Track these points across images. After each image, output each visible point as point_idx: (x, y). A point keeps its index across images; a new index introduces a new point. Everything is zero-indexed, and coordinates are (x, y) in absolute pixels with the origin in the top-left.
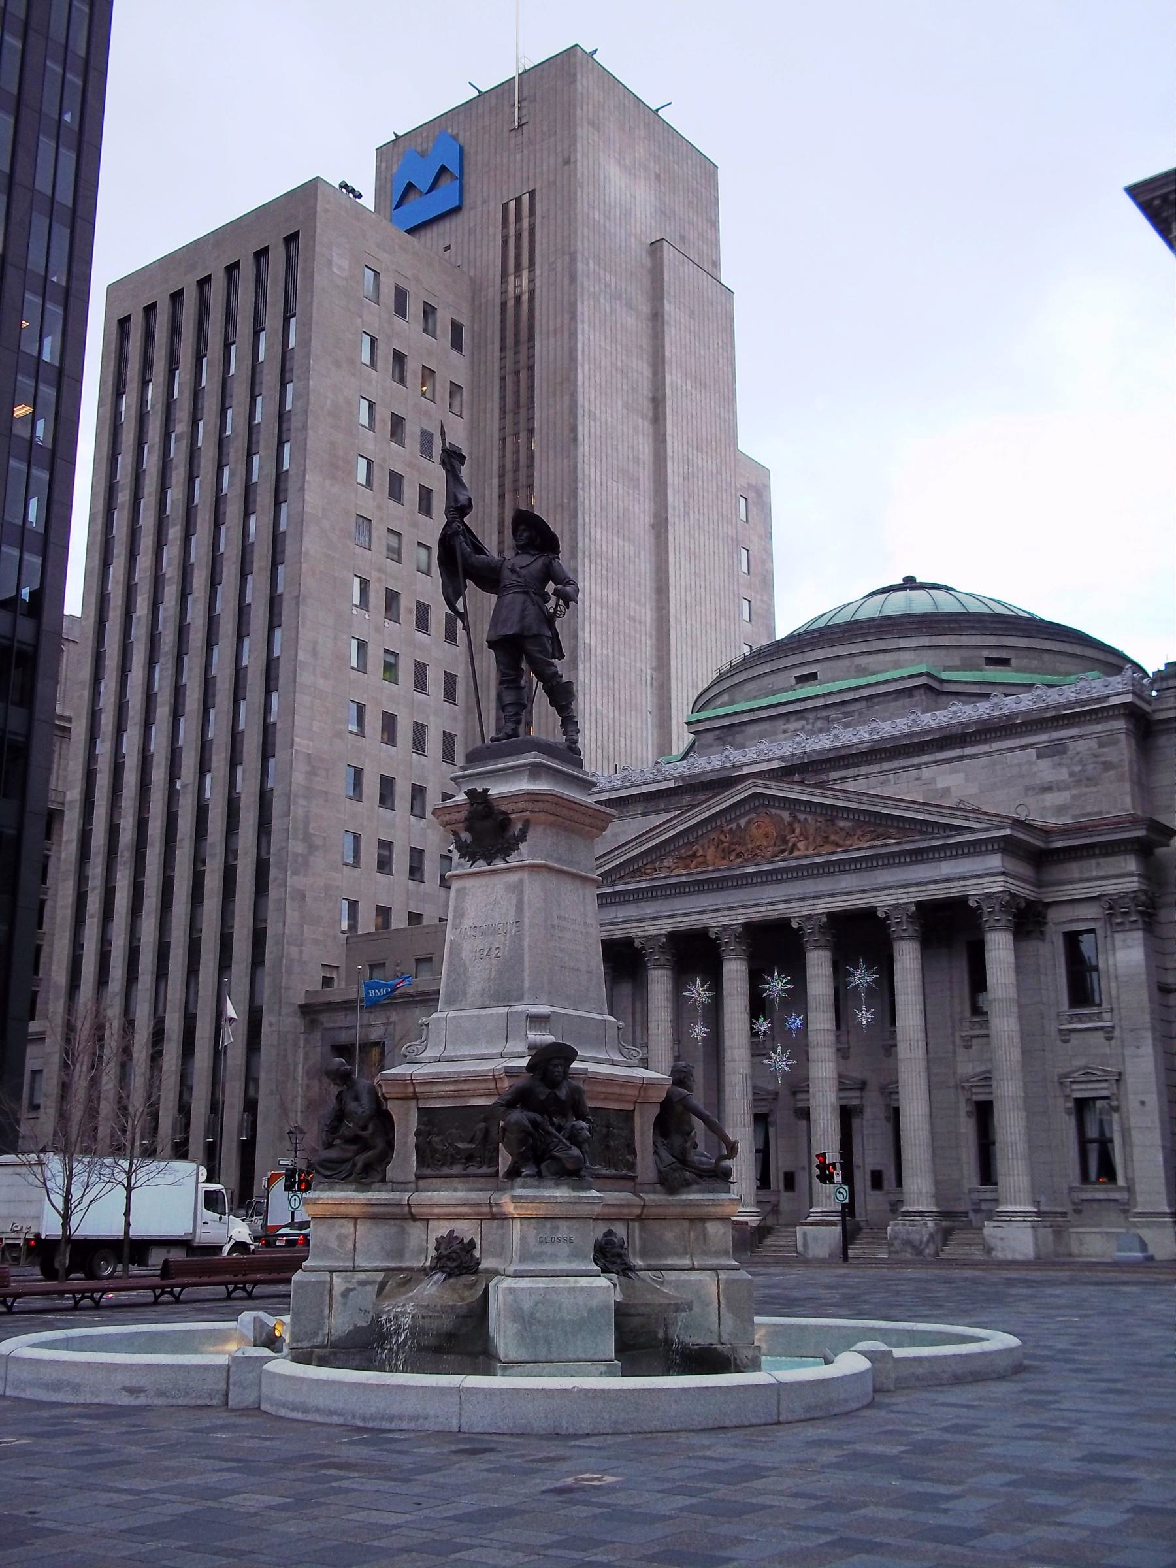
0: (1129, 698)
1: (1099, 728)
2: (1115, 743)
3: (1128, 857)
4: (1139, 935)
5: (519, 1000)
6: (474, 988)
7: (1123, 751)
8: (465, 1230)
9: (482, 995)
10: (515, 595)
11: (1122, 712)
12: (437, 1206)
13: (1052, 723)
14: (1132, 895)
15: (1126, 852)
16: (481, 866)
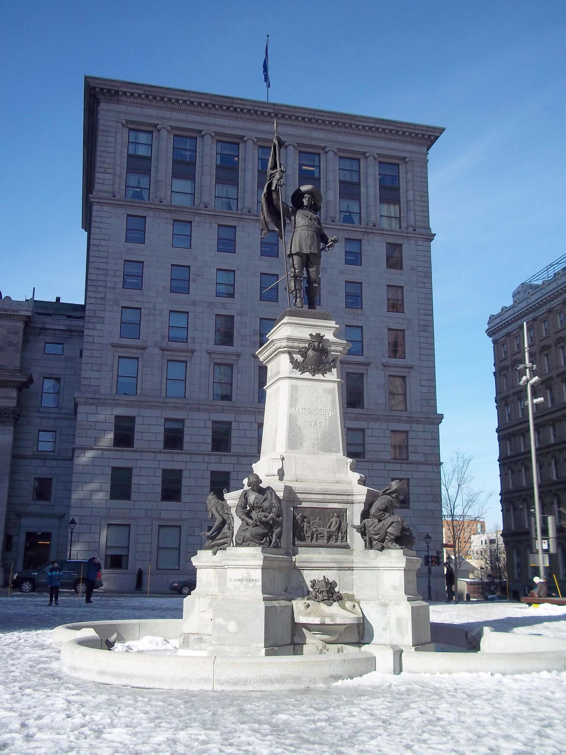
0: (29, 314)
1: (10, 324)
2: (16, 333)
3: (13, 390)
4: (12, 428)
5: (337, 453)
6: (307, 443)
7: (18, 338)
8: (331, 576)
9: (313, 448)
10: (314, 233)
11: (24, 319)
12: (314, 562)
13: (7, 317)
14: (12, 409)
15: (13, 387)
16: (307, 375)
